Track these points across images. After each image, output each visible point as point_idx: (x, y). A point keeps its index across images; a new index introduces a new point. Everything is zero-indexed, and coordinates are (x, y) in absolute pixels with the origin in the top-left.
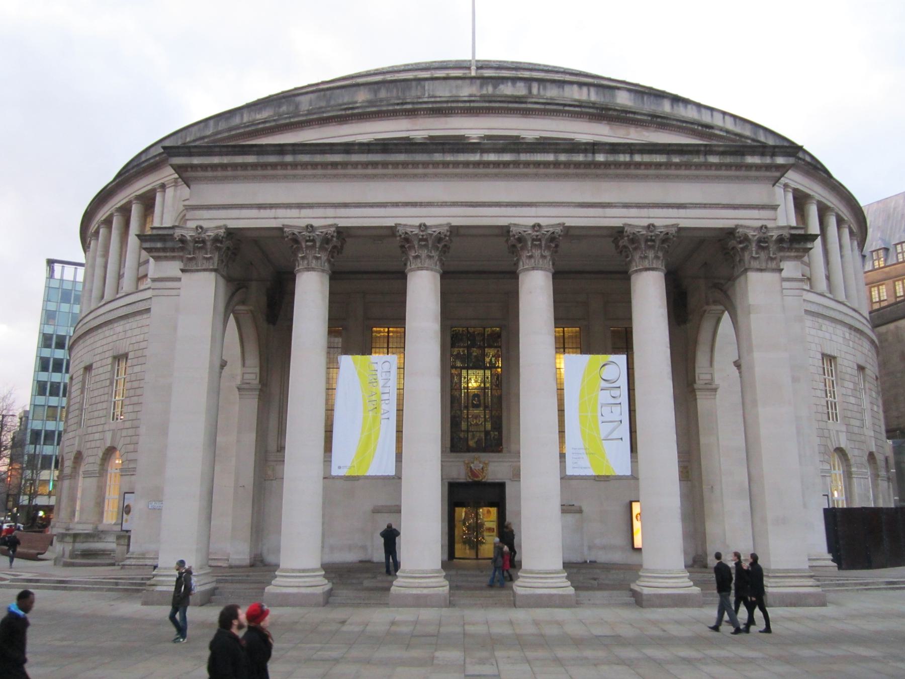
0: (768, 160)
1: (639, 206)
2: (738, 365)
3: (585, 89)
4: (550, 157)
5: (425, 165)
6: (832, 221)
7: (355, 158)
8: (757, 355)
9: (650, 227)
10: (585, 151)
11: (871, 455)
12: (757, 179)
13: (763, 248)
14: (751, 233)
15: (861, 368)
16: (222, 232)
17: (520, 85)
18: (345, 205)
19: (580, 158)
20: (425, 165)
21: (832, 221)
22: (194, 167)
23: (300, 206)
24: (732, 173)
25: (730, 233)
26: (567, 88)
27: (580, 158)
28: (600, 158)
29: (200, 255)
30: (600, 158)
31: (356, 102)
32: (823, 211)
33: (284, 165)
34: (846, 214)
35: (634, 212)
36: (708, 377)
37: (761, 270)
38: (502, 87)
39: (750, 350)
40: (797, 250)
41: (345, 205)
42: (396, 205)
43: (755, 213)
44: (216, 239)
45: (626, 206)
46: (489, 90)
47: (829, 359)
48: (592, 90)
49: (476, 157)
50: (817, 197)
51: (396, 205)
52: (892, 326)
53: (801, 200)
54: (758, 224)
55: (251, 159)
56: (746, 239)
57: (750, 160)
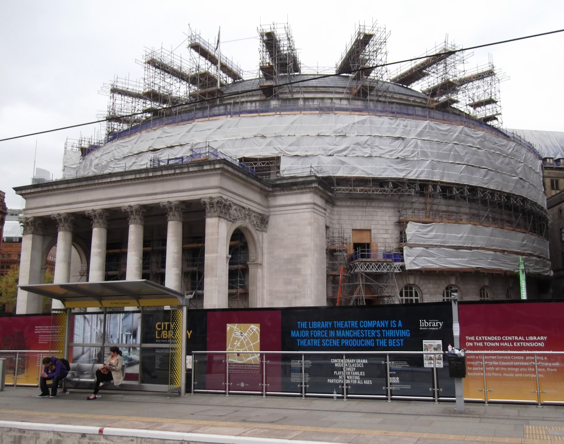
0: (212, 167)
1: (168, 193)
3: (254, 104)
4: (133, 177)
5: (95, 184)
10: (145, 172)
12: (213, 175)
13: (212, 207)
14: (207, 201)
18: (71, 204)
19: (143, 175)
23: (57, 205)
24: (199, 174)
27: (143, 175)
28: (151, 174)
33: (51, 190)
36: (254, 258)
37: (211, 217)
40: (309, 188)
41: (71, 204)
44: (31, 222)
48: (258, 104)
49: (108, 180)
56: (205, 204)
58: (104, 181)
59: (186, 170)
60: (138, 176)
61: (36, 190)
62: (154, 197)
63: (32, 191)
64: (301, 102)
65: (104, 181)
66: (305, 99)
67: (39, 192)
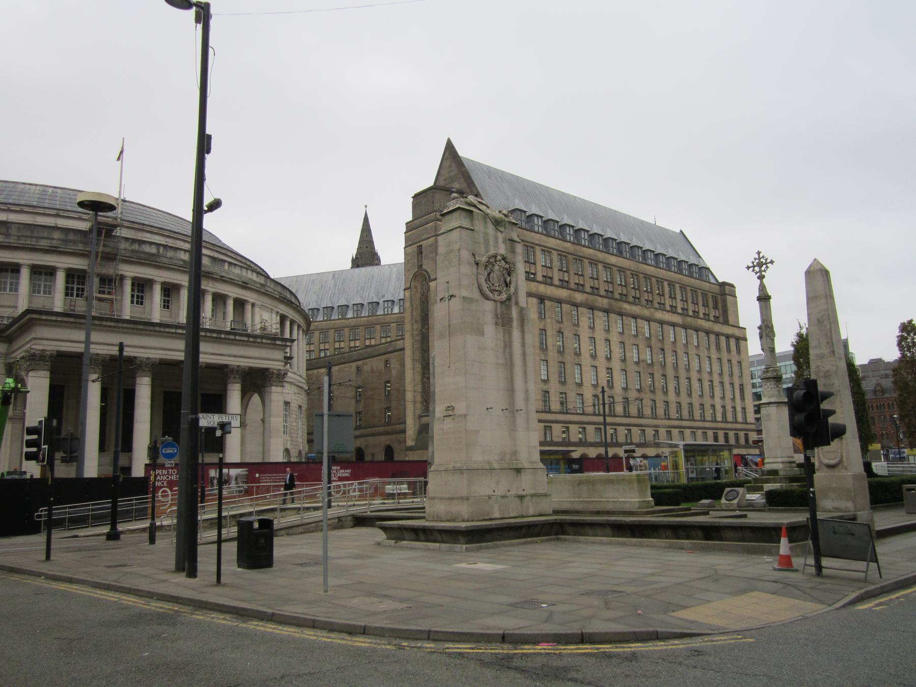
2: (263, 421)
5: (151, 331)
6: (296, 327)
7: (120, 325)
8: (272, 419)
9: (239, 366)
11: (300, 452)
15: (300, 407)
16: (55, 353)
17: (154, 246)
19: (215, 335)
20: (151, 331)
21: (296, 327)
22: (40, 319)
25: (267, 370)
26: (178, 252)
27: (215, 335)
28: (223, 336)
29: (41, 363)
30: (223, 336)
31: (53, 239)
32: (292, 322)
34: (303, 324)
35: (232, 359)
38: (143, 246)
39: (270, 416)
42: (135, 347)
43: (276, 363)
44: (51, 356)
45: (230, 356)
46: (136, 247)
47: (287, 404)
49: (173, 331)
50: (291, 317)
51: (135, 347)
52: (315, 371)
53: (283, 318)
54: (278, 368)
55: (72, 320)
56: (273, 373)
57: (278, 342)
58: (167, 330)
59: (259, 340)
60: (208, 334)
61: (66, 319)
62: (219, 357)
63: (59, 319)
64: (226, 265)
65: (167, 330)
66: (230, 263)
67: (71, 323)
